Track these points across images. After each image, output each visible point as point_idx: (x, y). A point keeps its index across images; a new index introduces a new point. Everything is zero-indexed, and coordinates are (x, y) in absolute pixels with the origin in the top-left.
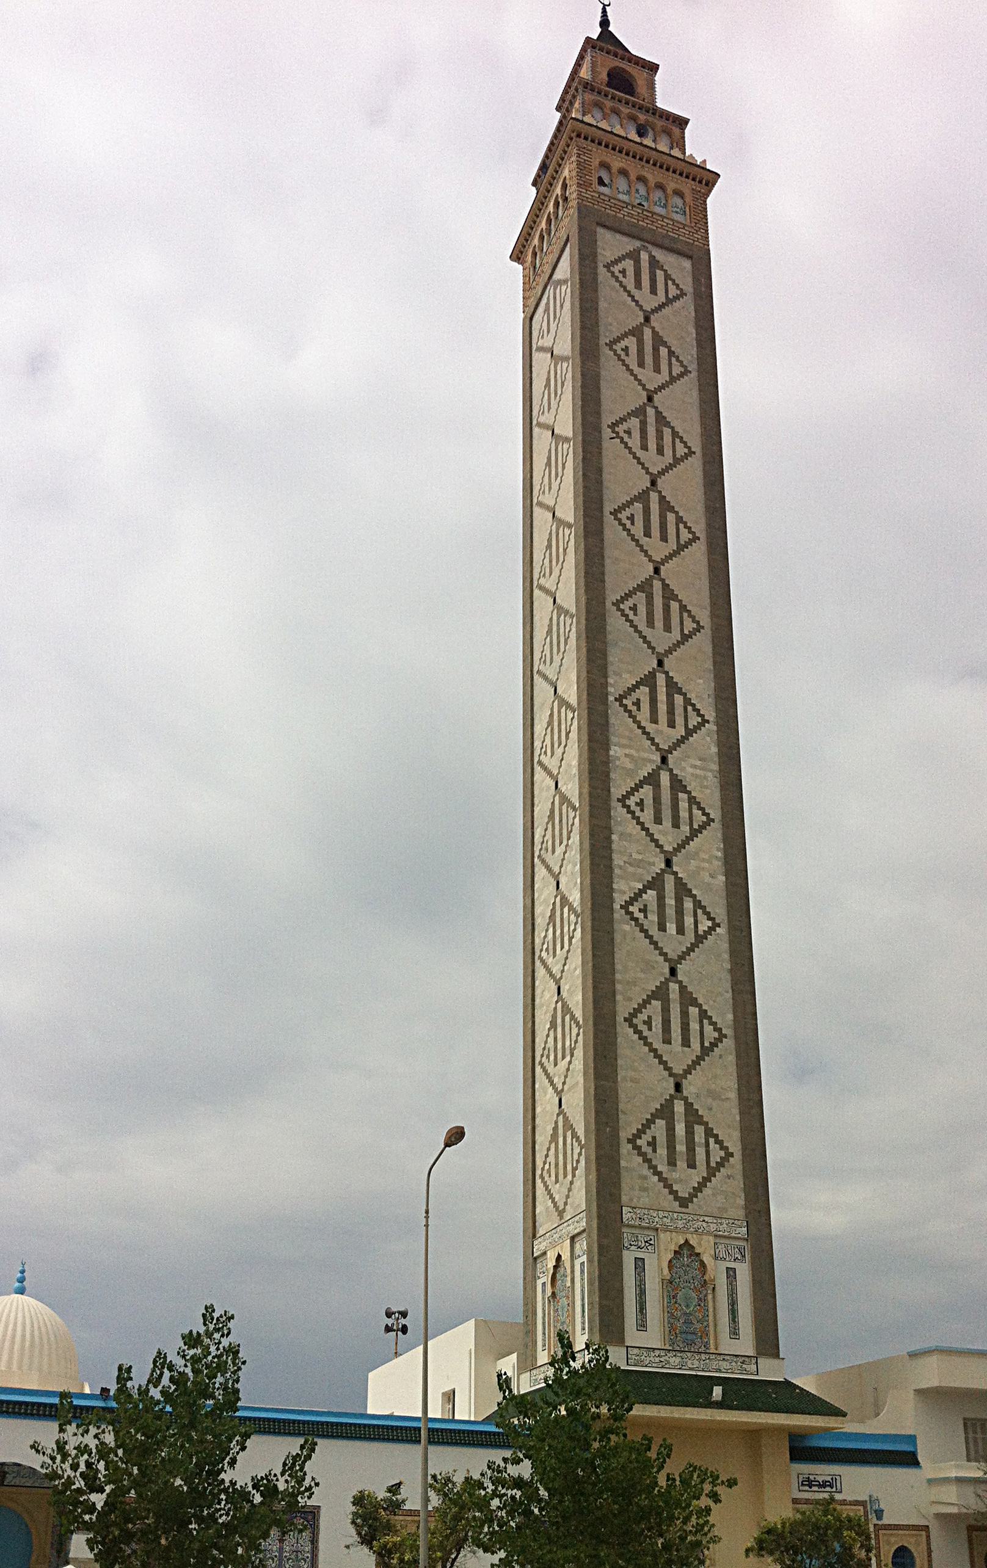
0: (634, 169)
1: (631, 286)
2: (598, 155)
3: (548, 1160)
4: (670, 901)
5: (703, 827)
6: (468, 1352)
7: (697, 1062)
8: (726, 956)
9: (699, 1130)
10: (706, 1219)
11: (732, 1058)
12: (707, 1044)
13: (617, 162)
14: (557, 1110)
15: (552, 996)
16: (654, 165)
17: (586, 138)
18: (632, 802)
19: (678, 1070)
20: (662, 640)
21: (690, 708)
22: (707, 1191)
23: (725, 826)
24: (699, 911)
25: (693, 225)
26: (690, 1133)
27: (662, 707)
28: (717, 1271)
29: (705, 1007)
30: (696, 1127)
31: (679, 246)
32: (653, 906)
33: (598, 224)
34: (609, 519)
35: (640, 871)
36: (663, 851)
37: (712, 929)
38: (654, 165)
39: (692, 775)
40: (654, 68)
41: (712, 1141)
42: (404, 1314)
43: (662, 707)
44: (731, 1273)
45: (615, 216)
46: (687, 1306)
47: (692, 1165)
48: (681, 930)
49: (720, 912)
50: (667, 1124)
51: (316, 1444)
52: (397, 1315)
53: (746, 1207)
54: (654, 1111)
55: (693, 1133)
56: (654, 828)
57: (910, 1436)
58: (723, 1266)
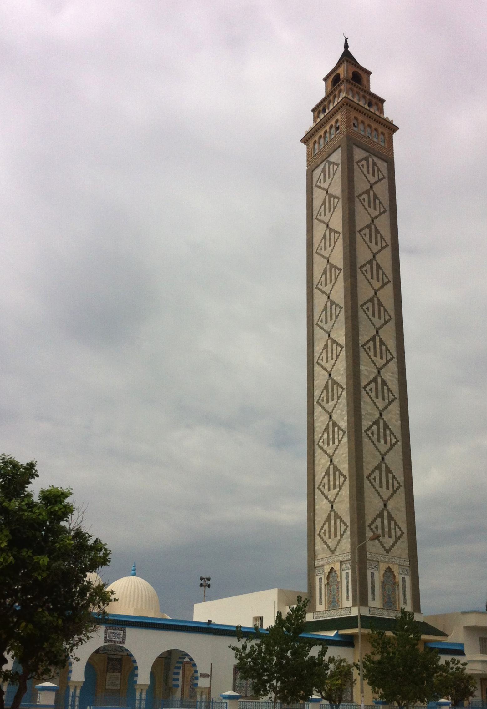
0: (367, 121)
1: (365, 173)
2: (354, 114)
3: (324, 529)
4: (382, 430)
5: (393, 401)
6: (273, 602)
7: (392, 495)
8: (401, 454)
9: (393, 523)
10: (396, 558)
11: (403, 495)
12: (395, 489)
13: (361, 118)
14: (330, 509)
15: (327, 462)
16: (375, 120)
17: (350, 106)
18: (368, 389)
19: (385, 498)
20: (378, 322)
21: (388, 352)
22: (395, 547)
23: (400, 400)
24: (392, 435)
25: (388, 148)
26: (389, 524)
27: (378, 350)
28: (399, 578)
29: (394, 474)
30: (391, 521)
31: (383, 157)
32: (376, 432)
33: (354, 144)
34: (358, 270)
35: (371, 417)
36: (379, 410)
37: (396, 442)
38: (375, 120)
39: (389, 379)
40: (369, 73)
41: (397, 527)
42: (209, 579)
43: (378, 350)
44: (404, 580)
45: (360, 141)
46: (389, 592)
47: (390, 537)
48: (385, 442)
49: (399, 436)
50: (381, 520)
51: (327, 648)
52: (205, 579)
53: (409, 554)
54: (377, 515)
55: (390, 524)
56: (376, 400)
57: (461, 644)
58: (402, 576)
